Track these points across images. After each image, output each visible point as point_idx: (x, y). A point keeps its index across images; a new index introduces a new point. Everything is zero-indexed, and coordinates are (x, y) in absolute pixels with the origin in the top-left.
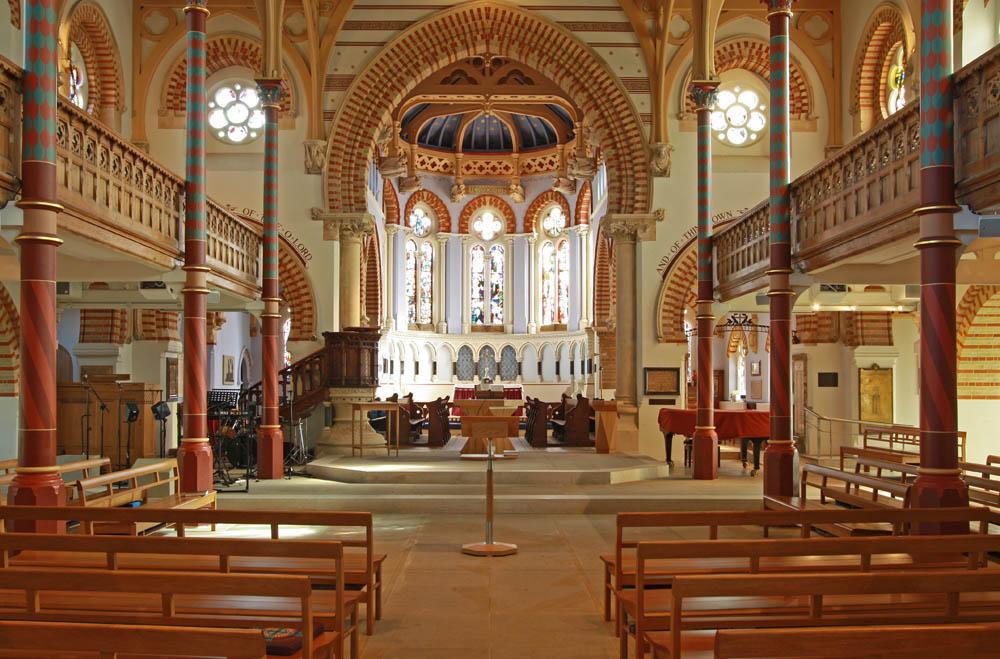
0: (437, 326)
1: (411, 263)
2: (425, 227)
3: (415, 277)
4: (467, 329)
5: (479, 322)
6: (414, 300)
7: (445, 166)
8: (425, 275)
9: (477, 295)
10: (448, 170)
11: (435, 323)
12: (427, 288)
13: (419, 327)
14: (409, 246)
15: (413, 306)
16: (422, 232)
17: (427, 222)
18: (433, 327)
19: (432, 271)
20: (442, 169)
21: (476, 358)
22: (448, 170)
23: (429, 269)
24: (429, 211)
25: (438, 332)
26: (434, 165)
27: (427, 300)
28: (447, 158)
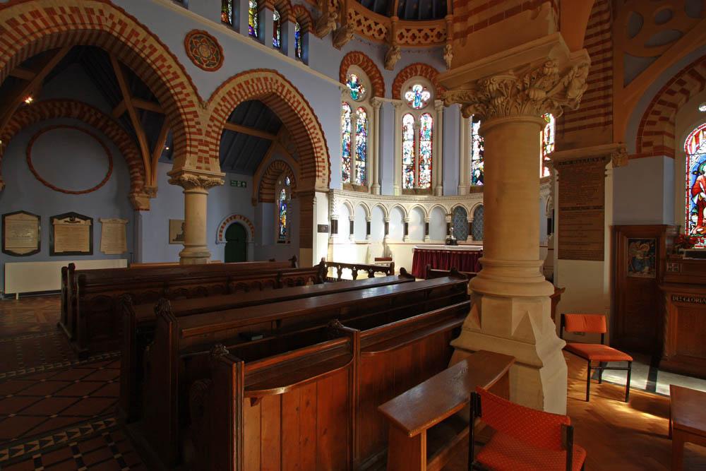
0: (435, 189)
1: (410, 134)
2: (425, 99)
3: (414, 147)
4: (463, 191)
5: (479, 183)
6: (411, 168)
7: (439, 35)
8: (426, 144)
9: (476, 156)
10: (442, 39)
11: (433, 188)
12: (427, 155)
13: (416, 191)
14: (408, 120)
15: (412, 173)
16: (421, 105)
17: (426, 96)
18: (430, 191)
19: (431, 140)
20: (436, 40)
21: (470, 218)
22: (442, 39)
23: (429, 139)
24: (428, 84)
25: (435, 195)
26: (426, 37)
27: (426, 167)
28: (438, 26)
